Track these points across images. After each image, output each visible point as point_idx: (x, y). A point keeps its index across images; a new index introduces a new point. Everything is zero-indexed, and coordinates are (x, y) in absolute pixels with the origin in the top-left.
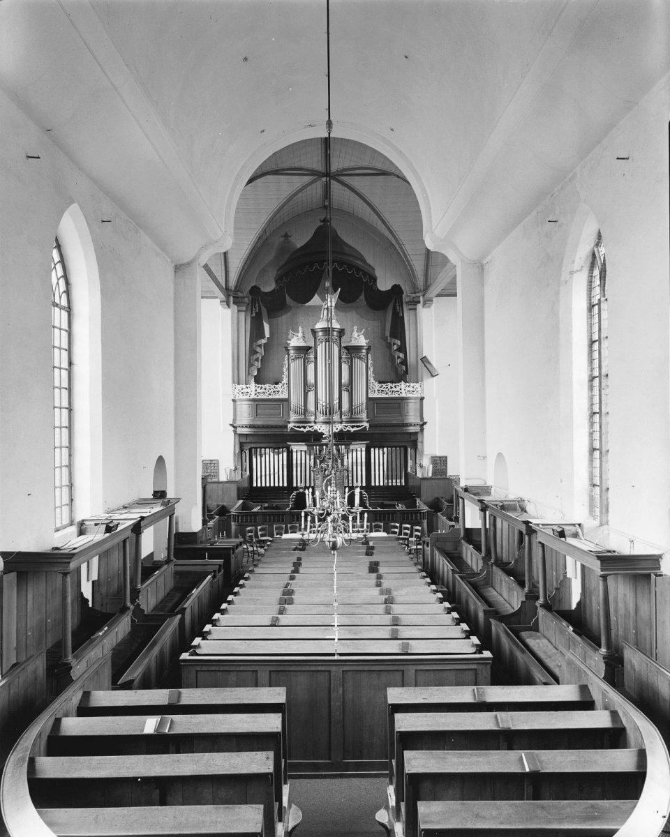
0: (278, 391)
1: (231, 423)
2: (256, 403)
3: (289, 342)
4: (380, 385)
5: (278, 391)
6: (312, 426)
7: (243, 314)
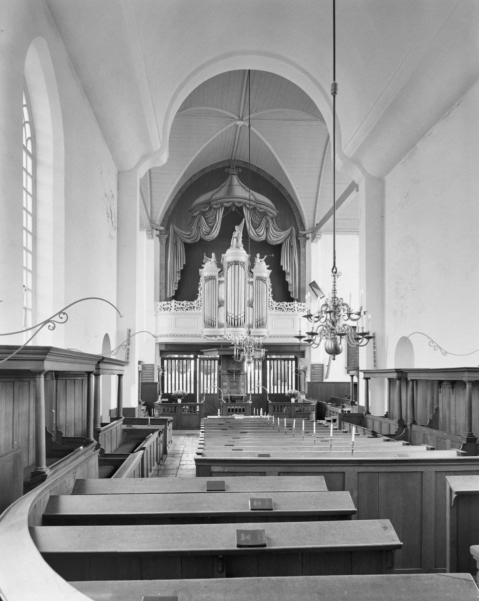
0: (194, 307)
2: (177, 316)
3: (203, 266)
4: (278, 303)
5: (194, 307)
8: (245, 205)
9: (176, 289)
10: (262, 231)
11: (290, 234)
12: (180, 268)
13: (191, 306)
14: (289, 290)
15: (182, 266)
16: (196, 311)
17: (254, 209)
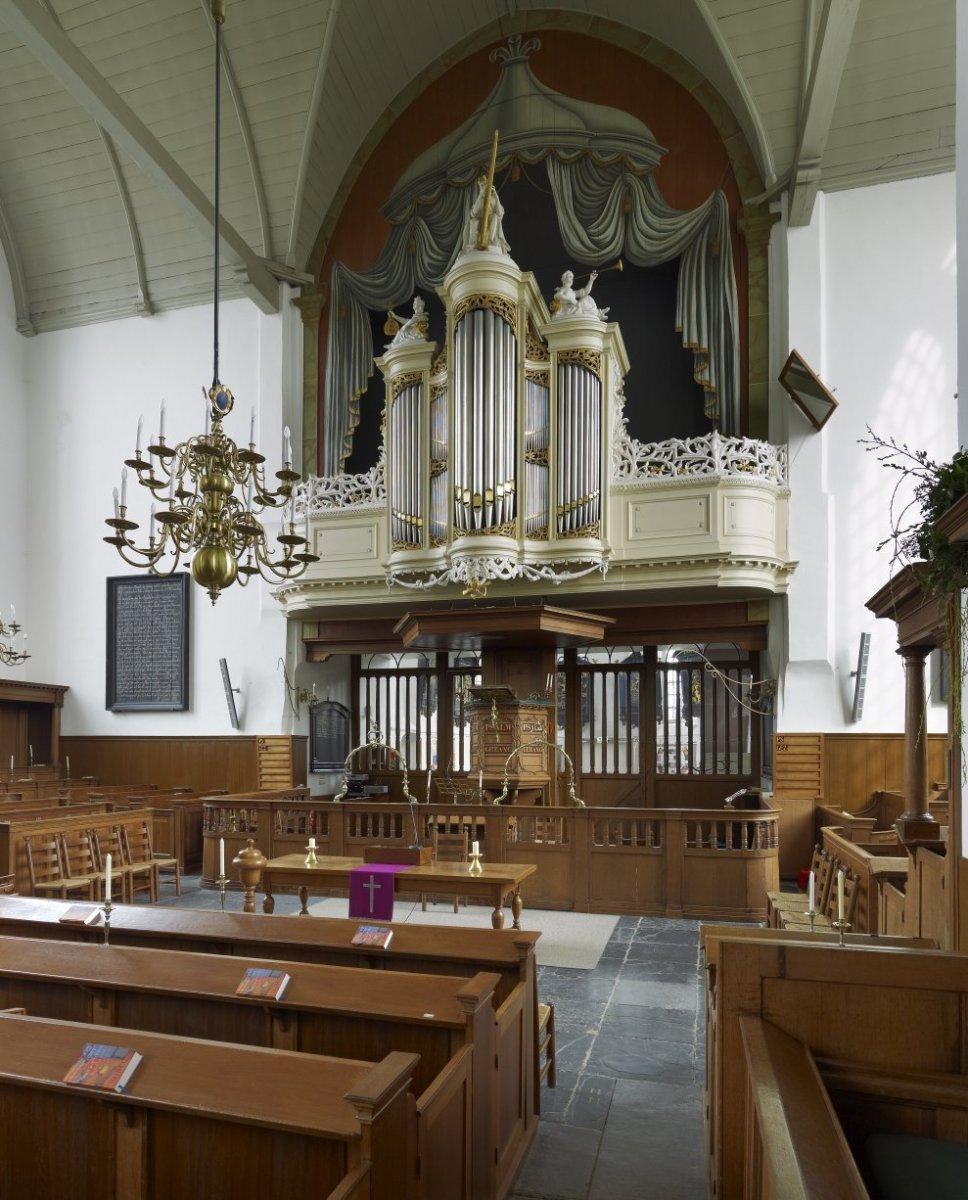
0: (368, 491)
4: (646, 448)
5: (368, 491)
6: (442, 572)
8: (552, 152)
9: (348, 455)
10: (610, 229)
11: (713, 217)
12: (358, 392)
13: (360, 487)
14: (707, 413)
15: (365, 382)
16: (377, 503)
17: (585, 156)
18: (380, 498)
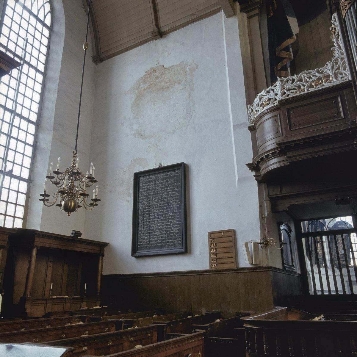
0: (329, 76)
1: (251, 161)
2: (288, 106)
5: (329, 76)
7: (256, 20)
18: (339, 79)
